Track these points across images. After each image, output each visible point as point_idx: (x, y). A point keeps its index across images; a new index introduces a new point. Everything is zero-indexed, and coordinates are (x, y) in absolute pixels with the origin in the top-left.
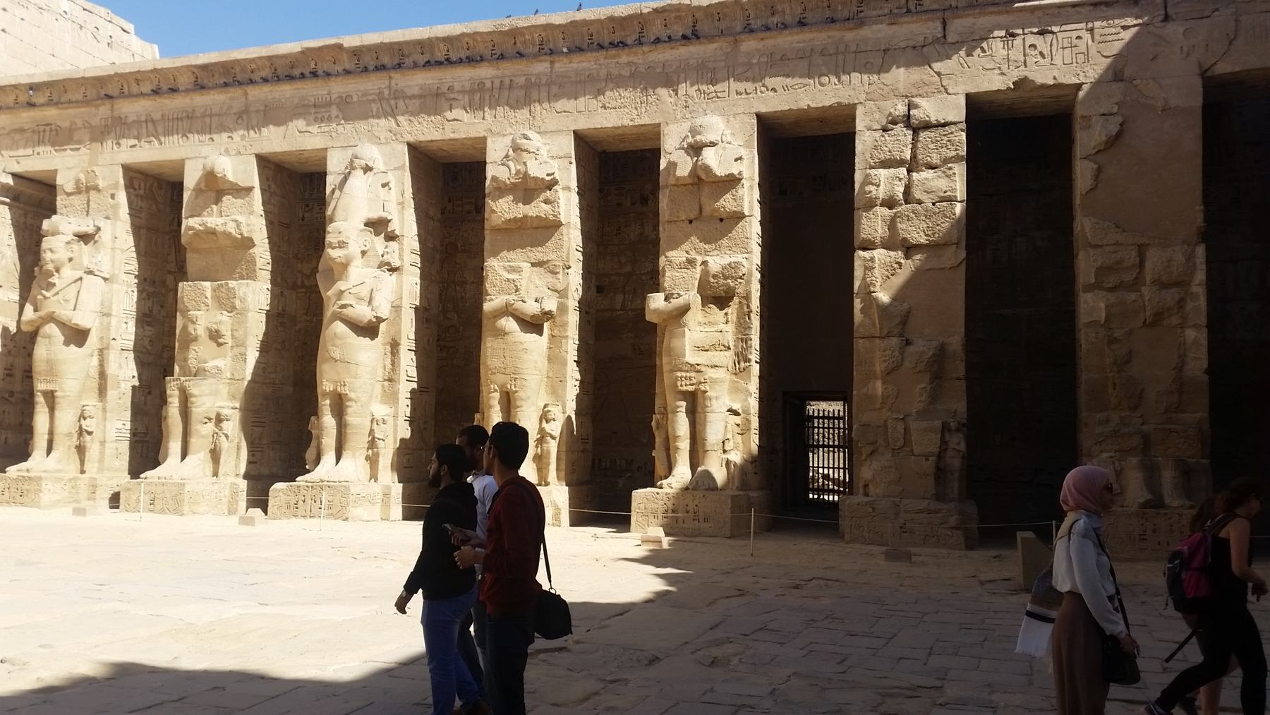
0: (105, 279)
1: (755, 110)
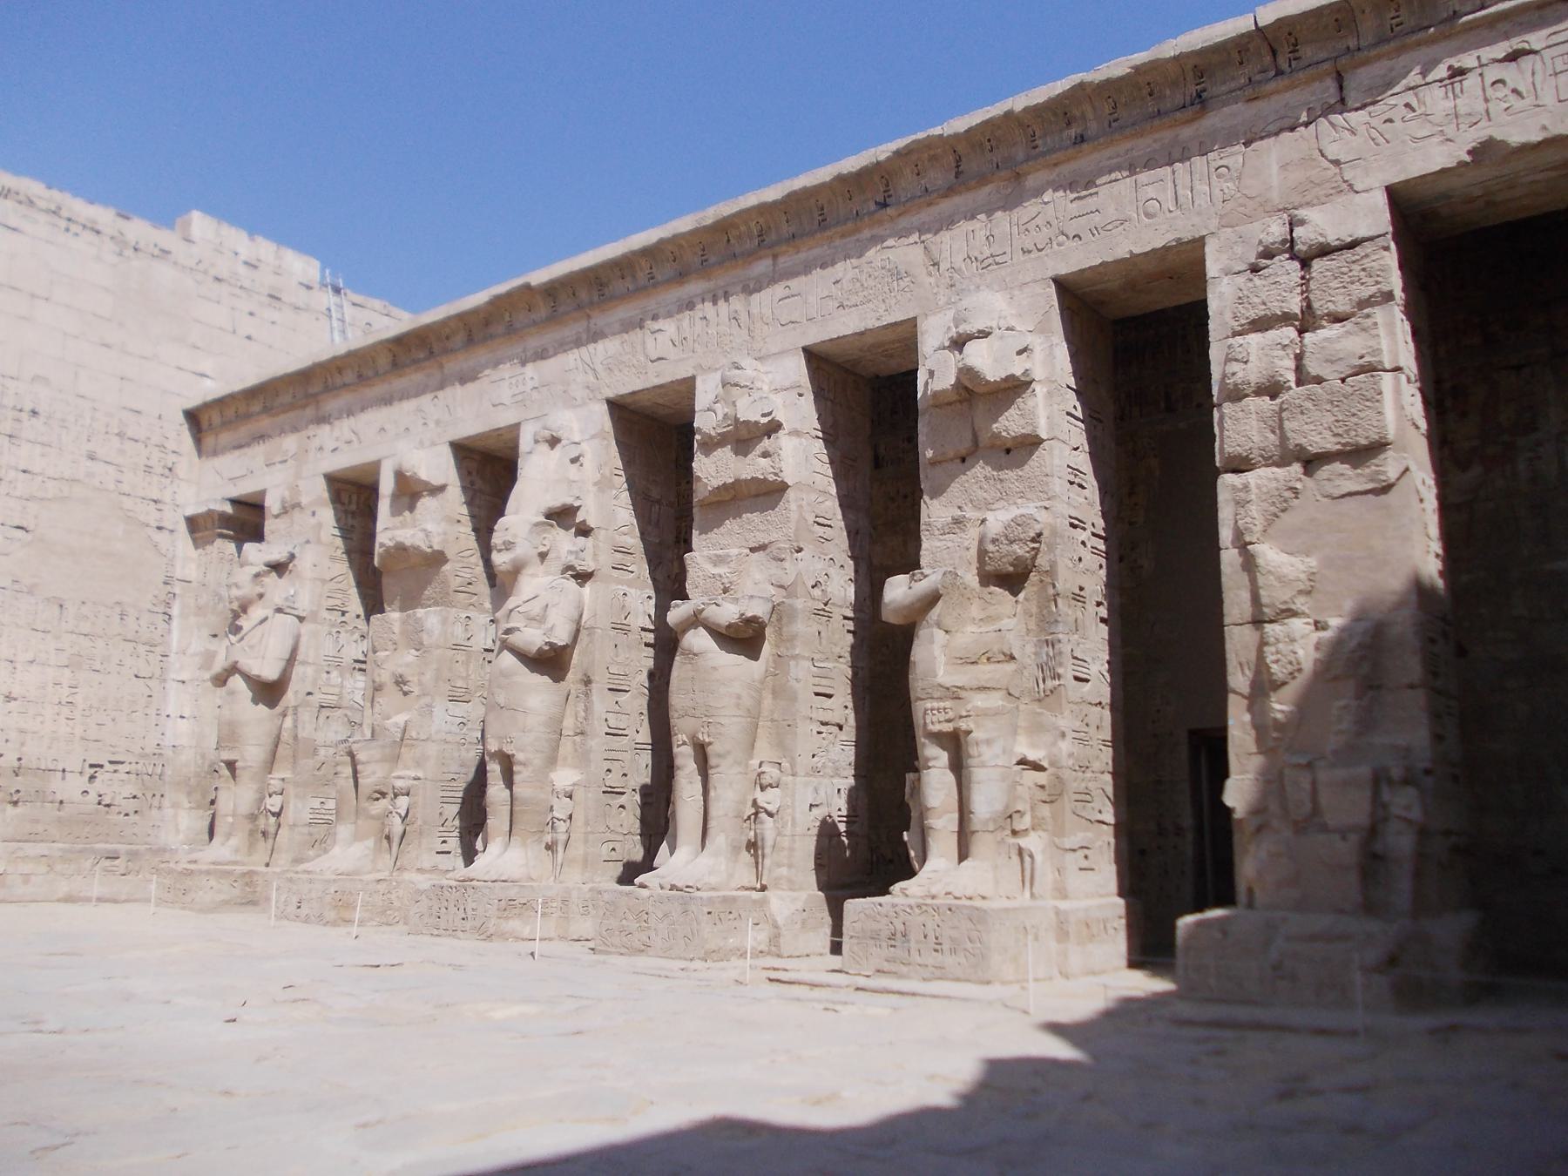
0: (301, 619)
1: (1051, 273)
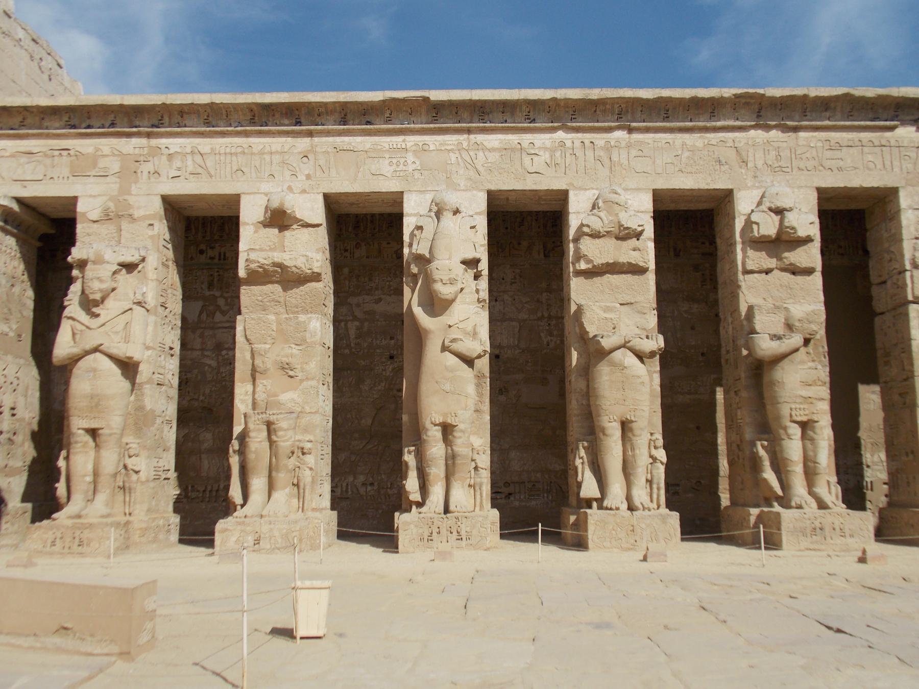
0: (148, 311)
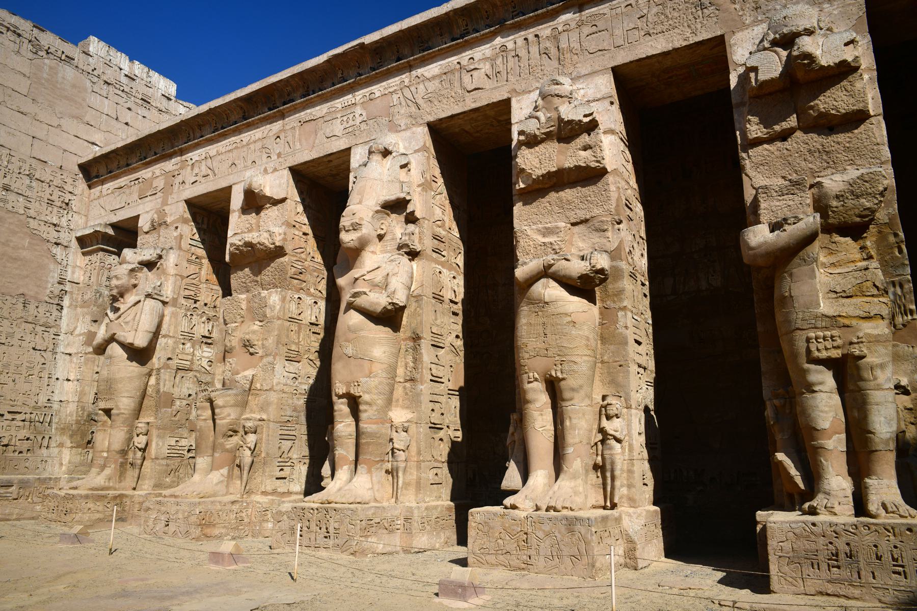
0: (164, 303)
